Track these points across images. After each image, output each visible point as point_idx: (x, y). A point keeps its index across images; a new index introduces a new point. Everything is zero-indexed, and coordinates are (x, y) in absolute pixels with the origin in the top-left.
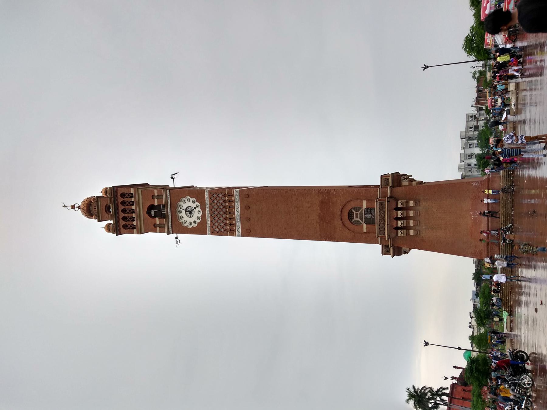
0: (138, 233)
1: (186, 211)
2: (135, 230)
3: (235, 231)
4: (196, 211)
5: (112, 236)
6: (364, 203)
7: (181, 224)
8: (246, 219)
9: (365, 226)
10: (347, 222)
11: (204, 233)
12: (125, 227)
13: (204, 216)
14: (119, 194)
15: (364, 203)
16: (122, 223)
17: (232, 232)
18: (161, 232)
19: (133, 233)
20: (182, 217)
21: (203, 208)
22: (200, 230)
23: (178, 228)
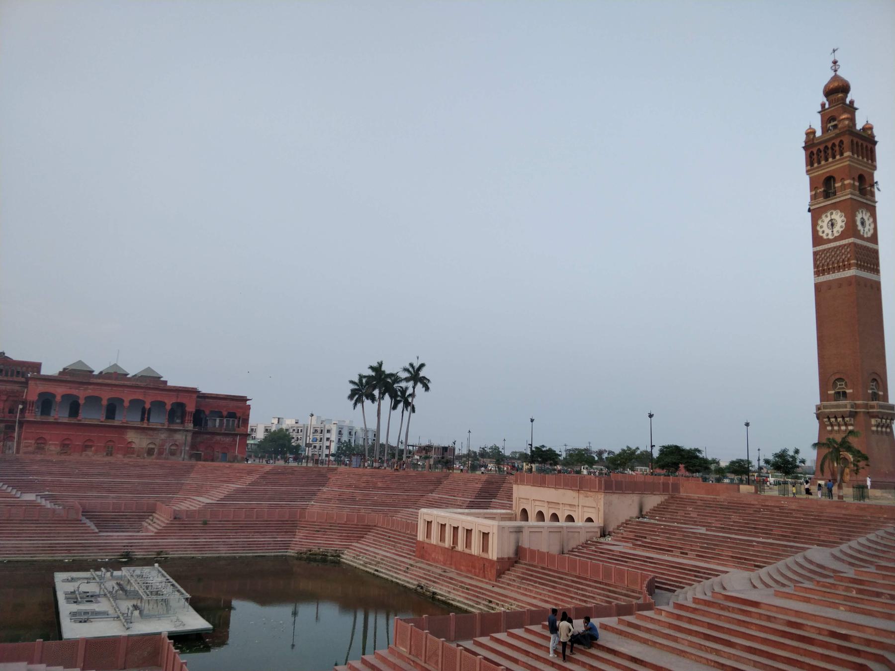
0: (807, 171)
1: (831, 220)
2: (809, 167)
3: (819, 276)
4: (830, 232)
5: (801, 140)
6: (851, 391)
7: (820, 217)
8: (829, 284)
9: (833, 392)
10: (837, 376)
11: (814, 245)
12: (812, 153)
13: (829, 241)
14: (842, 138)
15: (851, 391)
16: (815, 150)
17: (817, 273)
18: (811, 196)
19: (807, 166)
20: (823, 221)
21: (836, 239)
22: (817, 240)
23: (816, 214)
